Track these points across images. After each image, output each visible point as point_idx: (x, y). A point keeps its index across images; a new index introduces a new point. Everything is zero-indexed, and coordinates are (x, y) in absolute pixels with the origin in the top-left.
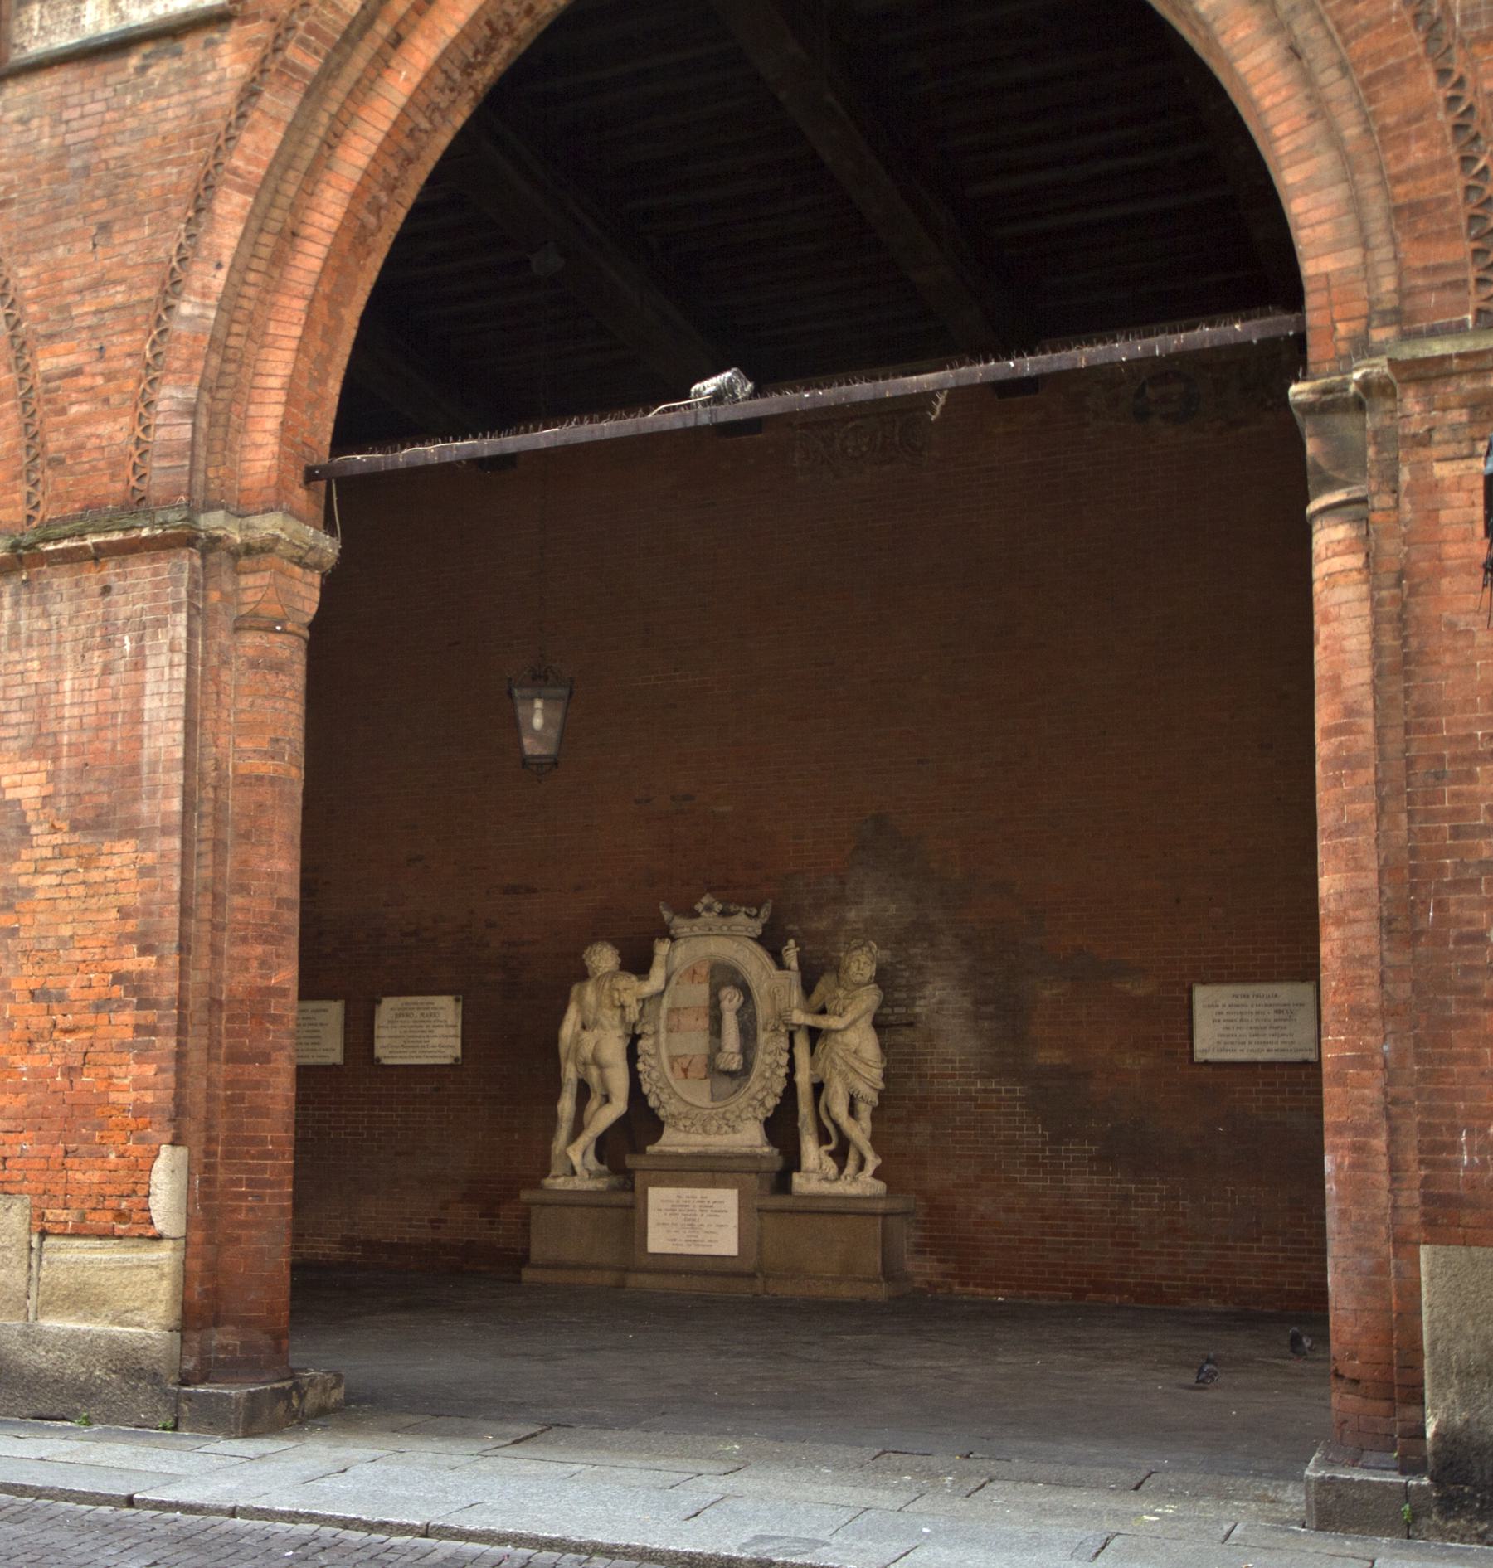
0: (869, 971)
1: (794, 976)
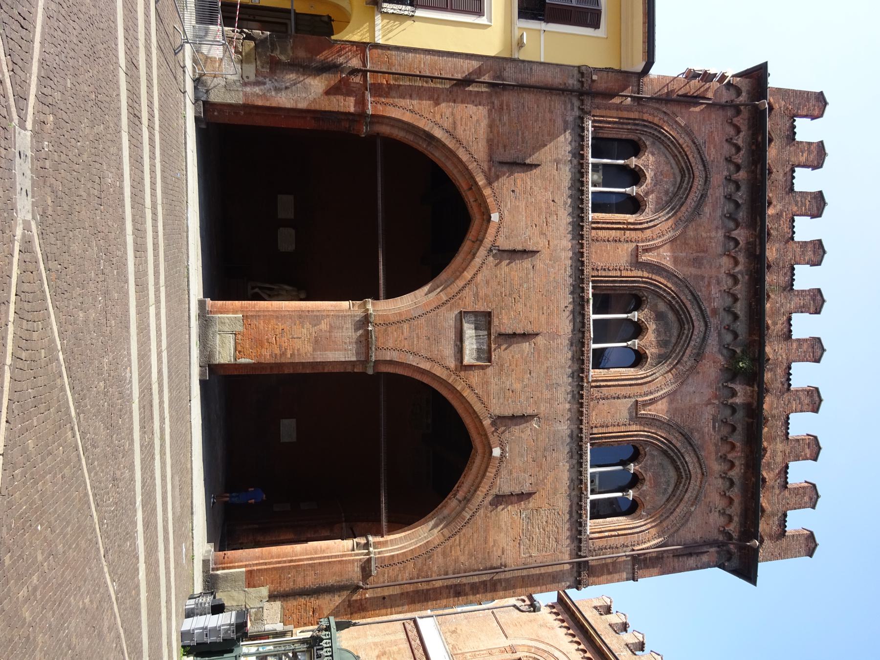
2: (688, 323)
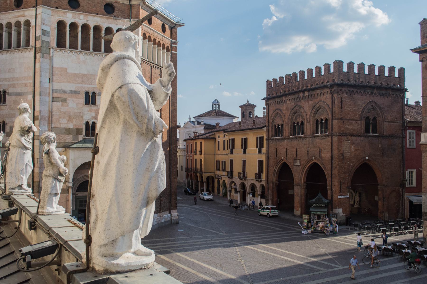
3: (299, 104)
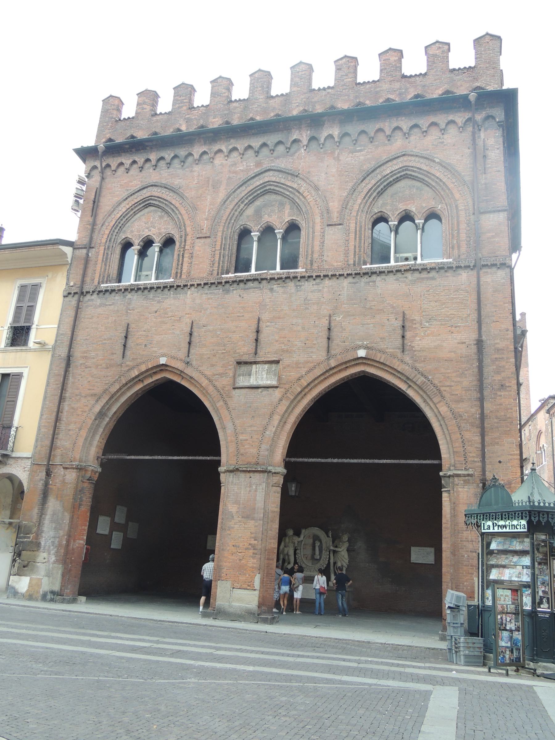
0: (347, 539)
1: (331, 539)
2: (265, 186)
3: (282, 164)
